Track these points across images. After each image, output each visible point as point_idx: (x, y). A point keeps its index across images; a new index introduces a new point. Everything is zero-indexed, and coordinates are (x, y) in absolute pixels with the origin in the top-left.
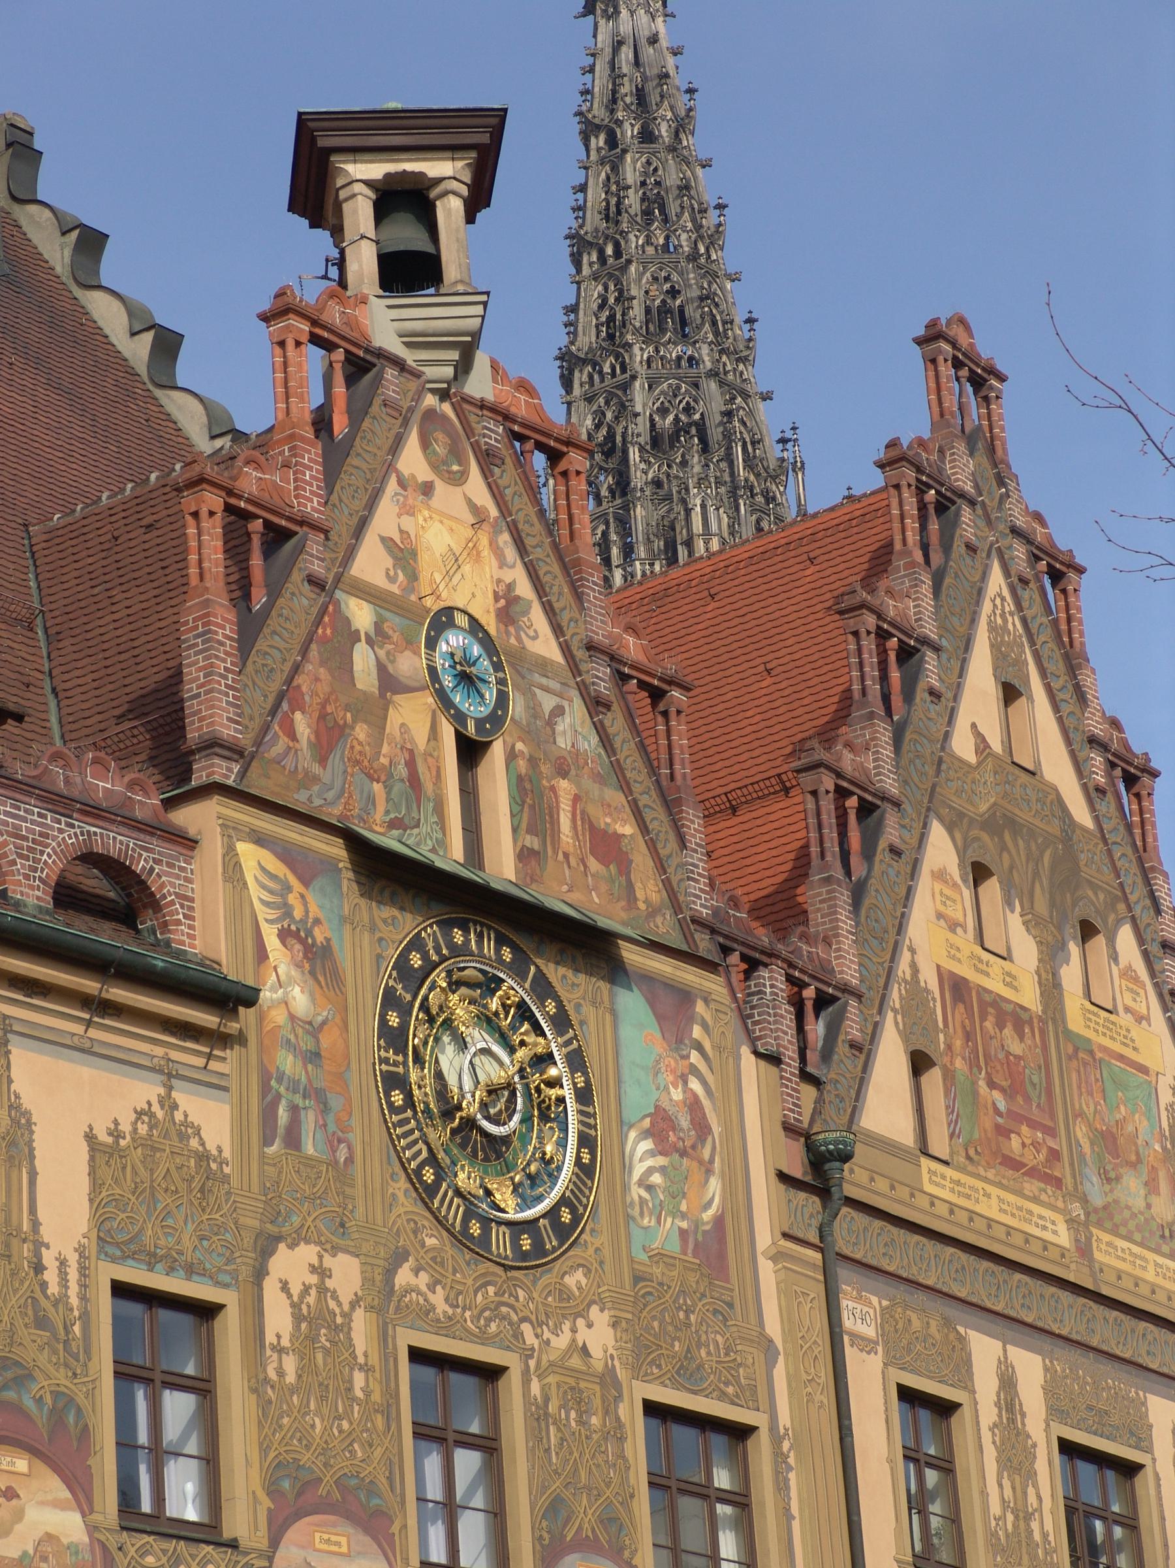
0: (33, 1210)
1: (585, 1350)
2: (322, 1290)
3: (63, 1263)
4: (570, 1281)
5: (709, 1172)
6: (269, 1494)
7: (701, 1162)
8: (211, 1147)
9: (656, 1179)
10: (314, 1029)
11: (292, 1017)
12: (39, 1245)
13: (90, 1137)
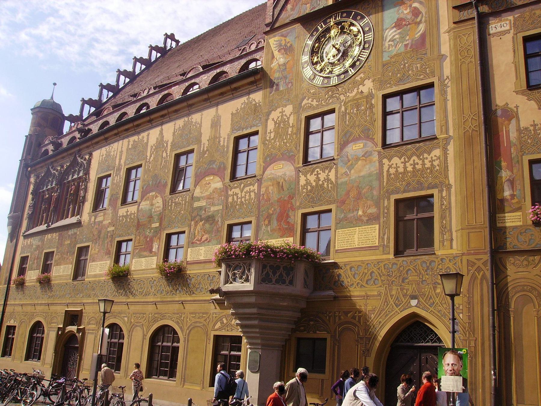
0: (219, 132)
1: (362, 92)
2: (282, 116)
3: (224, 139)
4: (358, 78)
5: (419, 23)
6: (264, 162)
7: (416, 23)
8: (257, 101)
9: (397, 36)
10: (285, 64)
11: (279, 65)
12: (220, 137)
13: (232, 114)
